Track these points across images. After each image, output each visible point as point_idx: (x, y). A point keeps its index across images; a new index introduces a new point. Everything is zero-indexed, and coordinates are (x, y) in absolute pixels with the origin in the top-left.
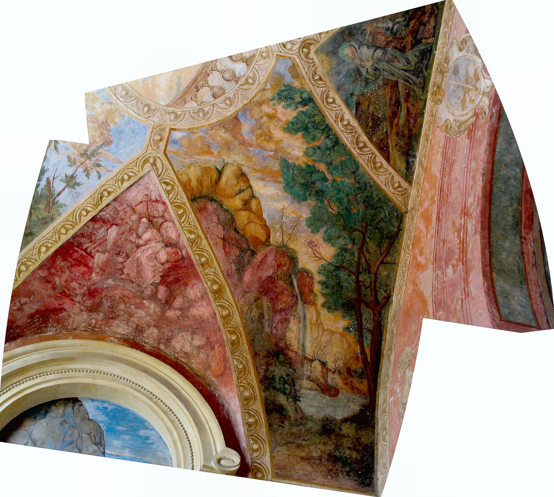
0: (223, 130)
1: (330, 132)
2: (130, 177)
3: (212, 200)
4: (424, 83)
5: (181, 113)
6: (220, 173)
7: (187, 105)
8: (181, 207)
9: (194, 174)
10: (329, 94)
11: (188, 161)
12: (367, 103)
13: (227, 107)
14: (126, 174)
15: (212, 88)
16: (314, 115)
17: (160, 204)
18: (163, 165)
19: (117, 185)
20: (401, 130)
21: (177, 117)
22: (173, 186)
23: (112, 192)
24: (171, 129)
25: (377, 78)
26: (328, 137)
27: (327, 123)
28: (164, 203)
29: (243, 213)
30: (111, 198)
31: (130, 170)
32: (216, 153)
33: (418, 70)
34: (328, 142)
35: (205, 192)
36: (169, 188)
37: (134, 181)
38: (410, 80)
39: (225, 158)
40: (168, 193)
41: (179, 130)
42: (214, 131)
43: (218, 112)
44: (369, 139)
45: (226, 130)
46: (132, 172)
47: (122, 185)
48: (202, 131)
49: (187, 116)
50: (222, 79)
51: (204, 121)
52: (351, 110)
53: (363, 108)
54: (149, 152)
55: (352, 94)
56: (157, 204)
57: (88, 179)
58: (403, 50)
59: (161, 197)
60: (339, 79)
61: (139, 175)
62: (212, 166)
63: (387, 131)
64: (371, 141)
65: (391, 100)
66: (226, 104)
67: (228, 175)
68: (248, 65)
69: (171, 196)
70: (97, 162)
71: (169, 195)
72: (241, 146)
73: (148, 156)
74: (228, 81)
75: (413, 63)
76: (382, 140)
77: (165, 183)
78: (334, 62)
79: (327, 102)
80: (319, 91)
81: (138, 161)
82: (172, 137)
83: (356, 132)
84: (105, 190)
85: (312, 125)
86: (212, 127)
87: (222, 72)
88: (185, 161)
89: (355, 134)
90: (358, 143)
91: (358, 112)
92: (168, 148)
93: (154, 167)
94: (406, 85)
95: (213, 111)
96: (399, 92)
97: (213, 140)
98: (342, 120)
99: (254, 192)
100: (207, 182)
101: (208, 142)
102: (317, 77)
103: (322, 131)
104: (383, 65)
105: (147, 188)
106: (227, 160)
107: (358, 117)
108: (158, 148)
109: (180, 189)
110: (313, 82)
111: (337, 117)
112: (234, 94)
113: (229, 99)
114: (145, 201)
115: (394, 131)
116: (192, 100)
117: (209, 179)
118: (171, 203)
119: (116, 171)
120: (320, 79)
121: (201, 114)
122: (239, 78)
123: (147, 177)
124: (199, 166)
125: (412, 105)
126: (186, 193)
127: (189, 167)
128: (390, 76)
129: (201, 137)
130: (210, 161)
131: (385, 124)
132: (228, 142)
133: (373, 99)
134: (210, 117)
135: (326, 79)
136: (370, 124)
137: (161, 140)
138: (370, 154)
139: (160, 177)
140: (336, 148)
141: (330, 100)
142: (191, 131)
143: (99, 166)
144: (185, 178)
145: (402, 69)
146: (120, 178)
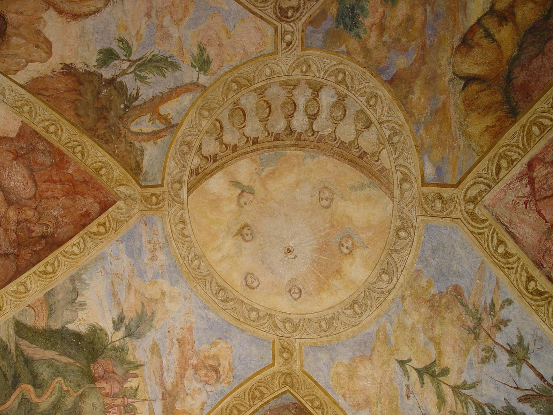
0: (411, 96)
2: (500, 242)
3: (509, 79)
5: (399, 173)
6: (469, 80)
7: (387, 166)
8: (529, 130)
9: (478, 125)
11: (462, 142)
13: (379, 101)
14: (497, 250)
15: (358, 133)
17: (535, 175)
18: (474, 184)
19: (515, 266)
21: (405, 179)
22: (501, 157)
23: (527, 273)
24: (424, 184)
28: (530, 166)
29: (519, 16)
30: (536, 272)
31: (490, 244)
32: (443, 98)
35: (498, 97)
36: (504, 164)
37: (504, 232)
39: (447, 79)
40: (512, 162)
41: (422, 169)
42: (415, 111)
43: (388, 113)
45: (410, 91)
46: (492, 240)
47: (512, 255)
48: (418, 130)
49: (401, 162)
50: (344, 121)
51: (404, 132)
54: (459, 215)
56: (537, 180)
57: (510, 321)
59: (520, 177)
61: (495, 225)
62: (462, 97)
66: (376, 103)
67: (470, 66)
68: (321, 88)
69: (515, 156)
70: (488, 309)
71: (515, 160)
72: (427, 59)
73: (466, 215)
74: (345, 111)
77: (498, 173)
81: (476, 231)
82: (433, 180)
84: (527, 289)
86: (409, 115)
87: (336, 122)
88: (462, 147)
92: (449, 182)
93: (479, 199)
95: (388, 121)
97: (426, 108)
99: (485, 11)
100: (485, 98)
101: (431, 116)
105: (515, 204)
106: (450, 76)
108: (451, 199)
109: (503, 141)
112: (362, 95)
113: (368, 101)
114: (536, 204)
116: (379, 159)
117: (480, 94)
118: (526, 152)
119: (496, 272)
121: (396, 139)
122: (340, 95)
123: (497, 210)
124: (465, 120)
126: (506, 129)
127: (468, 136)
129: (426, 130)
130: (455, 104)
132: (426, 83)
134: (397, 123)
137: (441, 198)
139: (491, 184)
142: (421, 149)
143: (493, 305)
144: (486, 138)
146: (503, 260)
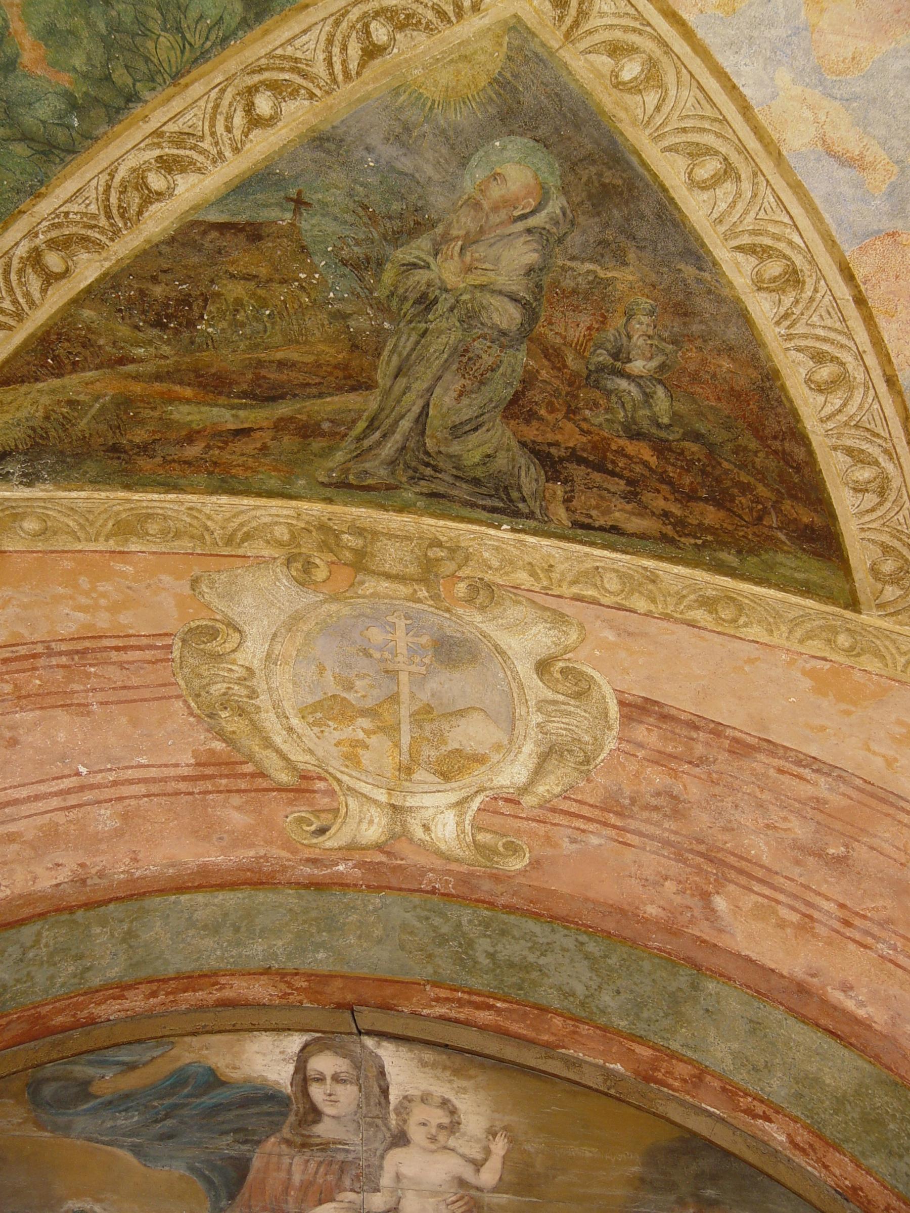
1: (98, 112)
4: (368, 488)
10: (294, 94)
12: (263, 271)
16: (179, 29)
20: (147, 413)
25: (382, 308)
26: (73, 105)
27: (146, 95)
33: (427, 465)
34: (45, 110)
38: (377, 435)
44: (89, 290)
52: (221, 201)
53: (235, 254)
55: (299, 203)
58: (516, 408)
60: (375, 139)
63: (133, 361)
64: (77, 301)
65: (281, 364)
75: (455, 448)
76: (86, 344)
78: (459, 117)
79: (252, 91)
80: (310, 48)
83: (116, 234)
85: (127, 19)
89: (102, 231)
90: (63, 244)
91: (214, 234)
94: (354, 422)
96: (321, 395)
98: (167, 165)
102: (380, 33)
103: (98, 73)
104: (446, 334)
107: (190, 234)
110: (355, 14)
111: (180, 139)
115: (137, 388)
120: (372, 52)
125: (264, 448)
128: (395, 361)
131: (166, 350)
133: (281, 293)
135: (374, 80)
136: (158, 291)
138: (15, 302)
140: (20, 149)
141: (264, 104)
145: (427, 405)
